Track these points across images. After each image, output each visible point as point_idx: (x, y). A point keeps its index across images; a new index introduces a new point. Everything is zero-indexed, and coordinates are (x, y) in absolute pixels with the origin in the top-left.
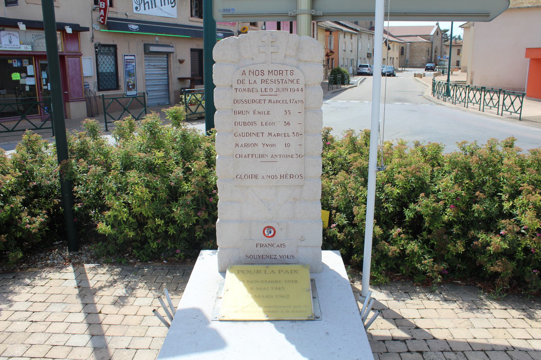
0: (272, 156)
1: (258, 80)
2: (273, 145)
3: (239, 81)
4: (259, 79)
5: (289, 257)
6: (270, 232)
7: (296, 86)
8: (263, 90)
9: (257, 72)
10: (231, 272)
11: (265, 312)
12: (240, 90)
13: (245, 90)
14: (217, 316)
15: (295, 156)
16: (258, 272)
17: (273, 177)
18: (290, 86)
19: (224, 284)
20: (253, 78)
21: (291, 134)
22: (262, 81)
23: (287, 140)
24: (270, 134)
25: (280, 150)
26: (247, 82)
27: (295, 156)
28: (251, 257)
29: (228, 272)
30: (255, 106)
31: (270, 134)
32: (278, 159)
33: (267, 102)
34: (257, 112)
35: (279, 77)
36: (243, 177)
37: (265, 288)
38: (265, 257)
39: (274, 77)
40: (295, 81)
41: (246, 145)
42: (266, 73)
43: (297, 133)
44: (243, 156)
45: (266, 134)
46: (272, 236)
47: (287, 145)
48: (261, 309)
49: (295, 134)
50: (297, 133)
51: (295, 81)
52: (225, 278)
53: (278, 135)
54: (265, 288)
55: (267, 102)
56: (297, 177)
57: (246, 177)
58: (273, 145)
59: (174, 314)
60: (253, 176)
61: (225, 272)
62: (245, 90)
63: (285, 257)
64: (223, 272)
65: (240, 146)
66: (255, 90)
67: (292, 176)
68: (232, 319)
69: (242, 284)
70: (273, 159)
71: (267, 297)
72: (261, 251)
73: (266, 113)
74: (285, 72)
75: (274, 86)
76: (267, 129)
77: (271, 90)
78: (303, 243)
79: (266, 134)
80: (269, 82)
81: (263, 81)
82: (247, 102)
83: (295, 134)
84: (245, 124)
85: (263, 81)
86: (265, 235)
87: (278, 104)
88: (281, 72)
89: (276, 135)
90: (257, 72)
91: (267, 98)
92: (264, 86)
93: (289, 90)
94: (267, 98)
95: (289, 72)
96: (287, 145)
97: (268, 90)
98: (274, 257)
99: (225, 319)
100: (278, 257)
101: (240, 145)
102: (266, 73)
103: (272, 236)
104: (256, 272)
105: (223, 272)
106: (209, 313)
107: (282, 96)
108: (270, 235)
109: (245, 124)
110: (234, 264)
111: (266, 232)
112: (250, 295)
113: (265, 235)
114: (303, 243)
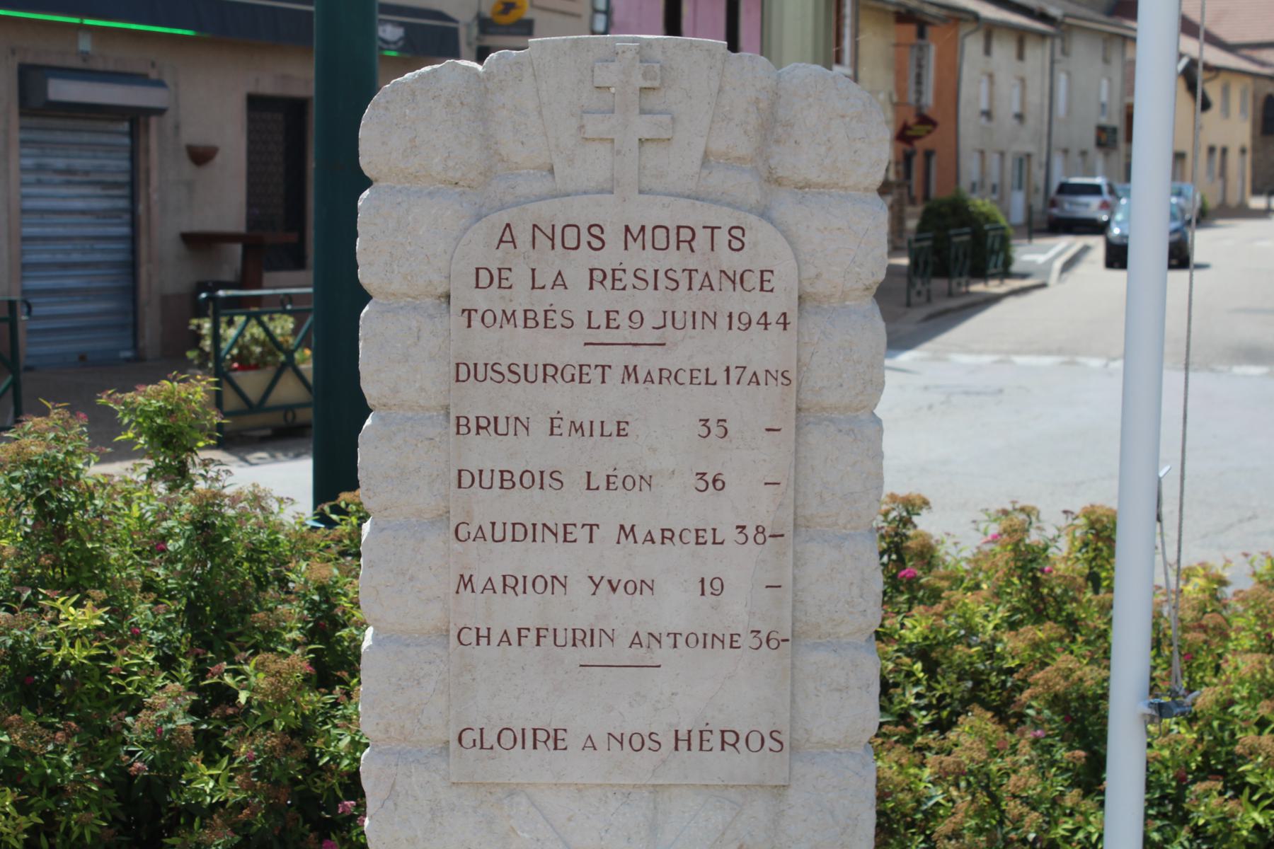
0: (636, 641)
1: (577, 275)
2: (643, 586)
4: (577, 265)
7: (754, 303)
9: (571, 234)
12: (489, 318)
13: (509, 317)
15: (746, 640)
17: (637, 742)
18: (731, 300)
20: (550, 261)
21: (728, 532)
22: (595, 278)
23: (710, 561)
24: (627, 532)
25: (674, 607)
26: (520, 277)
27: (746, 640)
30: (559, 396)
31: (627, 532)
32: (662, 653)
33: (615, 375)
35: (674, 259)
36: (490, 739)
39: (648, 260)
40: (753, 280)
41: (511, 584)
42: (613, 236)
43: (760, 530)
44: (495, 638)
45: (607, 532)
47: (711, 587)
49: (751, 531)
50: (760, 530)
51: (753, 280)
53: (667, 535)
55: (615, 375)
56: (755, 742)
57: (507, 738)
58: (643, 586)
60: (541, 736)
62: (509, 317)
65: (478, 589)
66: (557, 319)
67: (730, 738)
70: (638, 654)
73: (611, 428)
74: (703, 237)
75: (650, 302)
76: (612, 509)
77: (636, 318)
79: (607, 532)
80: (629, 279)
81: (598, 275)
82: (519, 373)
83: (751, 531)
84: (506, 480)
85: (598, 275)
87: (670, 388)
88: (686, 235)
89: (657, 536)
90: (571, 234)
91: (617, 357)
92: (602, 298)
93: (723, 321)
94: (617, 357)
95: (722, 237)
96: (711, 587)
97: (622, 319)
101: (479, 583)
102: (613, 236)
107: (688, 350)
109: (506, 480)
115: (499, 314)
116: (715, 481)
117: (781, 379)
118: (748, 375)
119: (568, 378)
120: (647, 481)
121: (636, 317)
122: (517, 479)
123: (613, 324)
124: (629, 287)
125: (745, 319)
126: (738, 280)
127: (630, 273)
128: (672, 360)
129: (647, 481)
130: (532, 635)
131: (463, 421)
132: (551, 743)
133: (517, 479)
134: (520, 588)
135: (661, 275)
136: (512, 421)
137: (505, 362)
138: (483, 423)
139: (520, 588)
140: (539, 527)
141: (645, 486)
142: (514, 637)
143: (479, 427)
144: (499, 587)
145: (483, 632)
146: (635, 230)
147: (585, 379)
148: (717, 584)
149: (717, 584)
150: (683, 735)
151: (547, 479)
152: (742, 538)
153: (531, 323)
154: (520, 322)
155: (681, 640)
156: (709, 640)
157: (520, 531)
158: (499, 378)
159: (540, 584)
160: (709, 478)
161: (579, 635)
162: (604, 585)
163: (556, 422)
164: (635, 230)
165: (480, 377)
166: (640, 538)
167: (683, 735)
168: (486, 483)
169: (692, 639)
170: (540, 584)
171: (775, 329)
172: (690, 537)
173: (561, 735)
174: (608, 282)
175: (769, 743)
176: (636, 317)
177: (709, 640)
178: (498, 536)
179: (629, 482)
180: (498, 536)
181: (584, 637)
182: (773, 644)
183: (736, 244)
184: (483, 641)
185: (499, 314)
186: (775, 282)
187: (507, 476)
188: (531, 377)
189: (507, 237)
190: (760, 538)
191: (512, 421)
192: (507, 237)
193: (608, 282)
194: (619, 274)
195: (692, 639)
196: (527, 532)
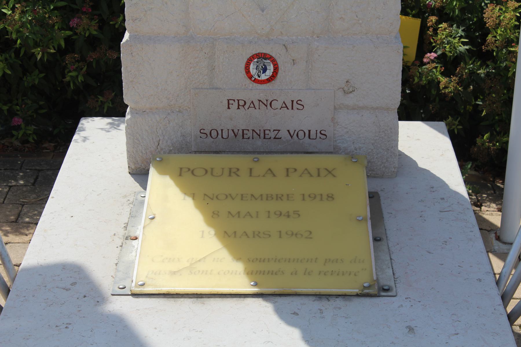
5: (313, 133)
6: (265, 70)
10: (162, 172)
11: (250, 273)
14: (127, 283)
16: (233, 172)
19: (142, 203)
28: (214, 134)
29: (153, 173)
37: (249, 214)
38: (250, 134)
48: (239, 267)
52: (145, 188)
54: (249, 214)
59: (13, 280)
61: (146, 173)
63: (301, 134)
64: (140, 174)
68: (164, 289)
69: (189, 202)
71: (256, 235)
72: (240, 119)
78: (350, 100)
86: (250, 77)
98: (272, 135)
99: (147, 289)
100: (283, 134)
104: (226, 172)
105: (140, 174)
106: (103, 275)
108: (264, 77)
110: (170, 152)
111: (252, 67)
112: (213, 232)
113: (250, 77)
114: (350, 100)
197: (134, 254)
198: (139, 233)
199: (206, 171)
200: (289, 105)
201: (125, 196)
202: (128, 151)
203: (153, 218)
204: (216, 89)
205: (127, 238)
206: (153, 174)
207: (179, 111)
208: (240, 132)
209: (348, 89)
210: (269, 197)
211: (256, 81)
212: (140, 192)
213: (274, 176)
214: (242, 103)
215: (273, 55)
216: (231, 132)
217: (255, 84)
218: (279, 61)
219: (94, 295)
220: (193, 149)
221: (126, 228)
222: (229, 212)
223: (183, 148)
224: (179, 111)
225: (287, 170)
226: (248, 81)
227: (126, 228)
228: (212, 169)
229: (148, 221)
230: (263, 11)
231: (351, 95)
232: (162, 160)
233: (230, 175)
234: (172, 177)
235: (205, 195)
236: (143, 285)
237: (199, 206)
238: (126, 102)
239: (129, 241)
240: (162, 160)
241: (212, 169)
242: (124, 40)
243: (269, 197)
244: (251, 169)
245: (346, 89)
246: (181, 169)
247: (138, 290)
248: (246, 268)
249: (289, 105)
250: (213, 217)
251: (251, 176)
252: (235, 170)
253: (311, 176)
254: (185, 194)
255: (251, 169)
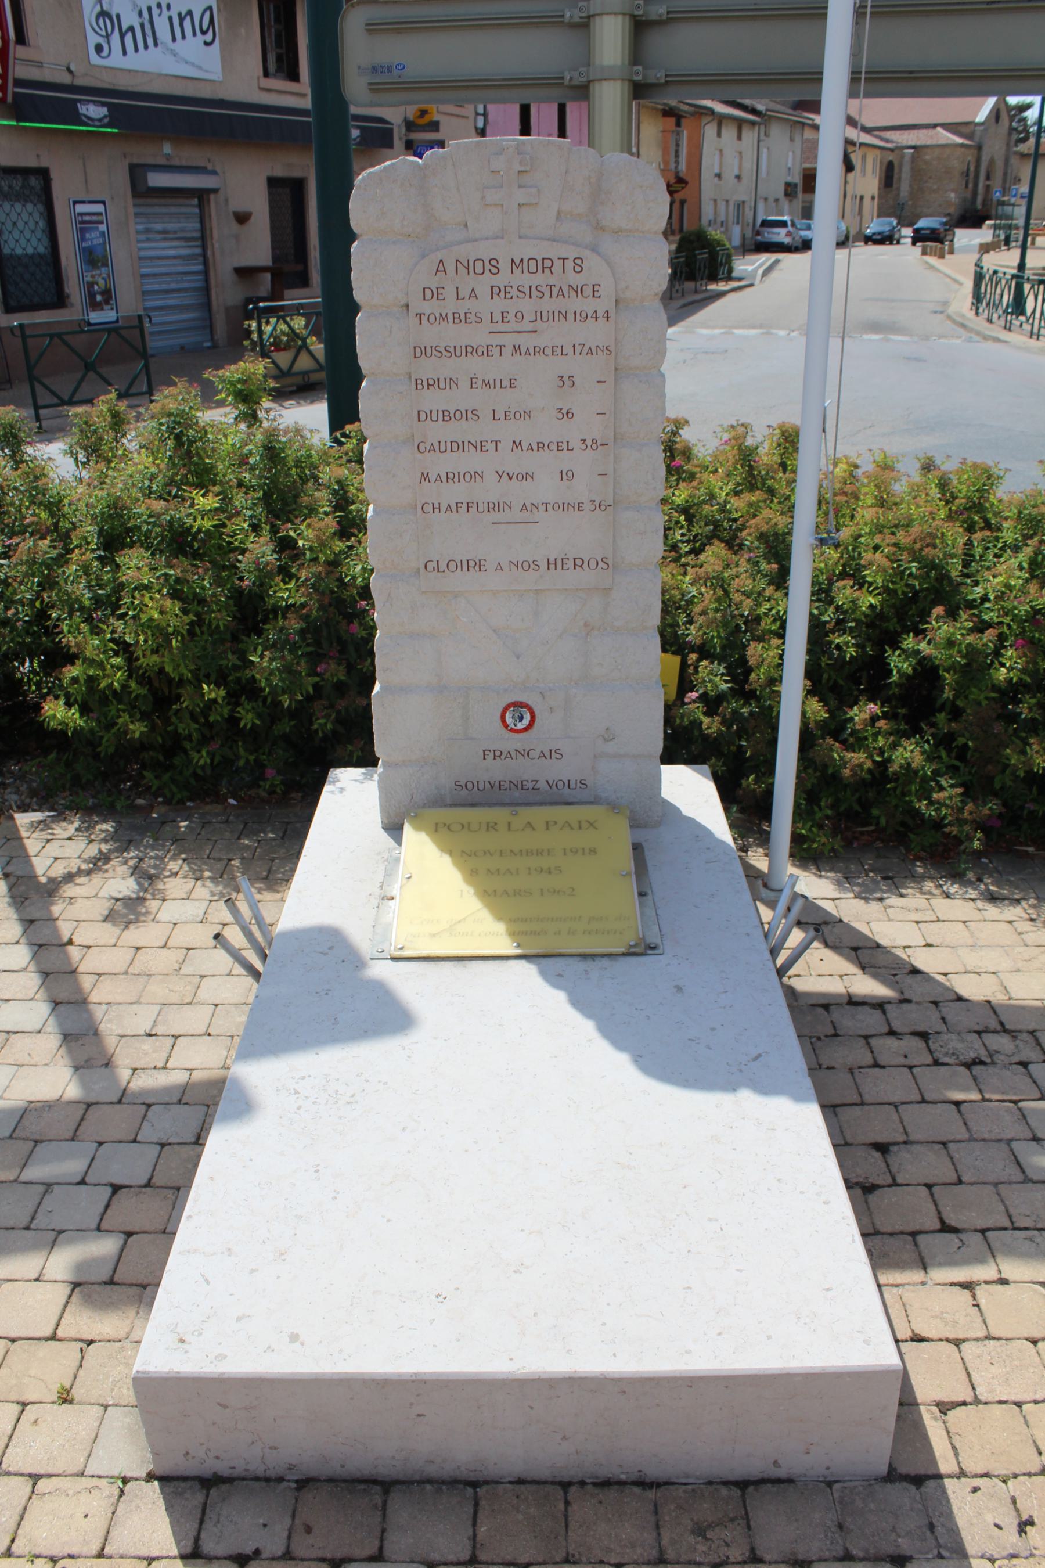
0: (524, 508)
1: (483, 291)
2: (527, 476)
3: (428, 292)
4: (483, 284)
5: (573, 785)
6: (521, 719)
7: (588, 305)
8: (497, 317)
9: (479, 264)
10: (418, 828)
11: (512, 934)
13: (444, 318)
14: (385, 947)
17: (526, 566)
18: (576, 304)
19: (398, 860)
20: (468, 282)
24: (517, 444)
25: (546, 487)
26: (449, 292)
28: (470, 785)
29: (407, 828)
30: (475, 365)
32: (540, 515)
33: (508, 351)
34: (479, 383)
35: (541, 279)
36: (443, 566)
37: (509, 871)
38: (507, 785)
39: (526, 280)
40: (588, 291)
41: (451, 477)
42: (504, 265)
44: (443, 509)
45: (506, 445)
46: (526, 729)
48: (501, 928)
49: (589, 443)
51: (588, 291)
53: (541, 446)
54: (509, 871)
55: (508, 351)
56: (593, 564)
57: (452, 565)
58: (527, 476)
59: (270, 944)
60: (472, 564)
61: (401, 828)
62: (444, 318)
63: (560, 784)
64: (394, 829)
65: (432, 480)
66: (473, 318)
68: (424, 953)
69: (446, 860)
71: (517, 893)
72: (497, 771)
74: (558, 264)
75: (527, 306)
77: (520, 316)
79: (506, 445)
80: (514, 292)
82: (452, 352)
83: (589, 443)
84: (446, 416)
87: (540, 358)
88: (547, 263)
89: (535, 447)
90: (479, 264)
91: (509, 340)
92: (499, 304)
94: (509, 340)
95: (569, 264)
97: (511, 317)
98: (530, 785)
99: (407, 953)
100: (542, 785)
101: (433, 478)
103: (526, 729)
105: (394, 829)
107: (550, 335)
109: (446, 416)
110: (424, 806)
112: (472, 890)
115: (438, 316)
116: (567, 413)
117: (605, 351)
118: (586, 348)
119: (480, 353)
120: (528, 414)
121: (519, 315)
122: (452, 415)
123: (505, 320)
124: (515, 296)
125: (584, 315)
126: (579, 291)
127: (515, 288)
128: (541, 341)
129: (528, 414)
130: (465, 506)
131: (419, 382)
132: (477, 568)
133: (452, 415)
134: (456, 479)
135: (533, 289)
136: (448, 381)
137: (443, 345)
138: (431, 382)
139: (456, 479)
140: (466, 444)
141: (527, 417)
142: (454, 508)
143: (429, 385)
144: (444, 479)
145: (437, 505)
146: (517, 262)
147: (490, 353)
148: (570, 474)
149: (570, 474)
150: (552, 561)
151: (470, 415)
152: (584, 447)
153: (457, 321)
154: (451, 320)
155: (550, 507)
156: (566, 507)
157: (455, 445)
158: (439, 354)
159: (468, 476)
160: (564, 412)
161: (491, 505)
162: (505, 475)
163: (474, 381)
164: (517, 262)
165: (428, 354)
166: (525, 448)
167: (552, 561)
168: (434, 418)
169: (556, 506)
170: (468, 476)
171: (602, 321)
172: (554, 447)
173: (482, 563)
174: (502, 294)
175: (601, 564)
176: (519, 315)
177: (566, 507)
178: (443, 449)
179: (518, 415)
180: (443, 449)
181: (495, 507)
182: (603, 508)
183: (578, 269)
184: (437, 511)
185: (438, 316)
186: (601, 291)
187: (446, 413)
188: (458, 354)
189: (441, 268)
190: (594, 447)
191: (448, 381)
192: (441, 268)
193: (502, 294)
194: (508, 289)
195: (556, 506)
196: (459, 446)
197: (391, 915)
198: (395, 891)
199: (463, 826)
200: (547, 755)
201: (379, 854)
202: (381, 806)
203: (409, 878)
204: (471, 739)
205: (383, 899)
206: (408, 829)
207: (434, 763)
208: (497, 783)
209: (608, 736)
210: (529, 853)
211: (512, 730)
212: (395, 849)
213: (534, 829)
214: (498, 753)
215: (530, 703)
216: (487, 784)
217: (511, 734)
218: (537, 713)
219: (353, 960)
220: (448, 802)
221: (381, 887)
222: (489, 870)
223: (438, 802)
224: (434, 763)
225: (547, 823)
226: (504, 730)
227: (381, 887)
228: (469, 824)
229: (405, 881)
230: (518, 658)
231: (611, 743)
232: (416, 815)
233: (488, 830)
234: (428, 834)
235: (463, 851)
236: (402, 948)
237: (456, 864)
238: (378, 755)
239: (385, 902)
240: (416, 815)
241: (469, 824)
242: (375, 692)
243: (529, 853)
244: (509, 824)
245: (606, 736)
246: (437, 824)
247: (397, 954)
248: (507, 930)
249: (547, 755)
250: (472, 875)
251: (509, 829)
252: (492, 824)
253: (572, 829)
254: (442, 850)
255: (509, 824)
